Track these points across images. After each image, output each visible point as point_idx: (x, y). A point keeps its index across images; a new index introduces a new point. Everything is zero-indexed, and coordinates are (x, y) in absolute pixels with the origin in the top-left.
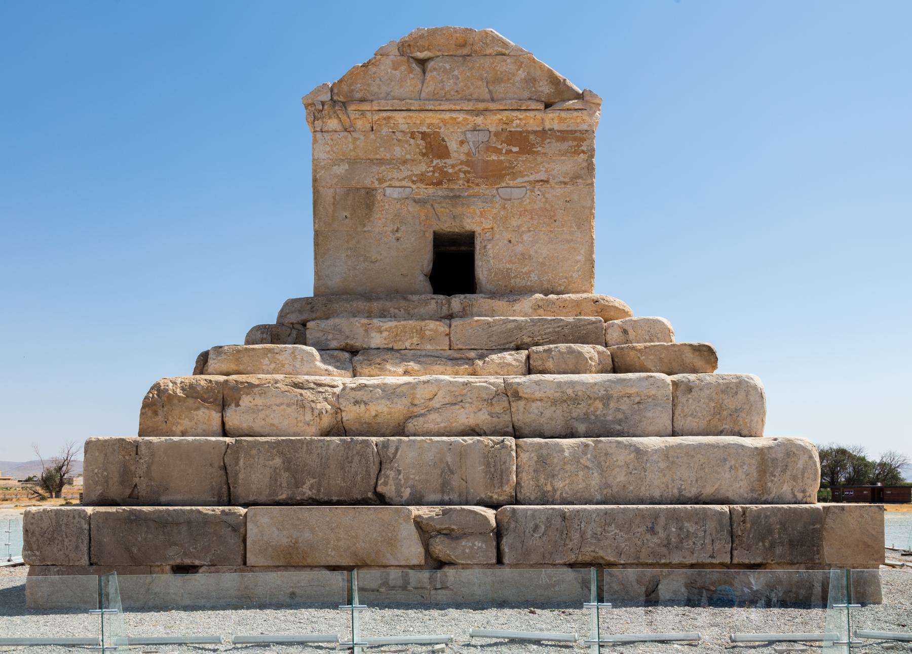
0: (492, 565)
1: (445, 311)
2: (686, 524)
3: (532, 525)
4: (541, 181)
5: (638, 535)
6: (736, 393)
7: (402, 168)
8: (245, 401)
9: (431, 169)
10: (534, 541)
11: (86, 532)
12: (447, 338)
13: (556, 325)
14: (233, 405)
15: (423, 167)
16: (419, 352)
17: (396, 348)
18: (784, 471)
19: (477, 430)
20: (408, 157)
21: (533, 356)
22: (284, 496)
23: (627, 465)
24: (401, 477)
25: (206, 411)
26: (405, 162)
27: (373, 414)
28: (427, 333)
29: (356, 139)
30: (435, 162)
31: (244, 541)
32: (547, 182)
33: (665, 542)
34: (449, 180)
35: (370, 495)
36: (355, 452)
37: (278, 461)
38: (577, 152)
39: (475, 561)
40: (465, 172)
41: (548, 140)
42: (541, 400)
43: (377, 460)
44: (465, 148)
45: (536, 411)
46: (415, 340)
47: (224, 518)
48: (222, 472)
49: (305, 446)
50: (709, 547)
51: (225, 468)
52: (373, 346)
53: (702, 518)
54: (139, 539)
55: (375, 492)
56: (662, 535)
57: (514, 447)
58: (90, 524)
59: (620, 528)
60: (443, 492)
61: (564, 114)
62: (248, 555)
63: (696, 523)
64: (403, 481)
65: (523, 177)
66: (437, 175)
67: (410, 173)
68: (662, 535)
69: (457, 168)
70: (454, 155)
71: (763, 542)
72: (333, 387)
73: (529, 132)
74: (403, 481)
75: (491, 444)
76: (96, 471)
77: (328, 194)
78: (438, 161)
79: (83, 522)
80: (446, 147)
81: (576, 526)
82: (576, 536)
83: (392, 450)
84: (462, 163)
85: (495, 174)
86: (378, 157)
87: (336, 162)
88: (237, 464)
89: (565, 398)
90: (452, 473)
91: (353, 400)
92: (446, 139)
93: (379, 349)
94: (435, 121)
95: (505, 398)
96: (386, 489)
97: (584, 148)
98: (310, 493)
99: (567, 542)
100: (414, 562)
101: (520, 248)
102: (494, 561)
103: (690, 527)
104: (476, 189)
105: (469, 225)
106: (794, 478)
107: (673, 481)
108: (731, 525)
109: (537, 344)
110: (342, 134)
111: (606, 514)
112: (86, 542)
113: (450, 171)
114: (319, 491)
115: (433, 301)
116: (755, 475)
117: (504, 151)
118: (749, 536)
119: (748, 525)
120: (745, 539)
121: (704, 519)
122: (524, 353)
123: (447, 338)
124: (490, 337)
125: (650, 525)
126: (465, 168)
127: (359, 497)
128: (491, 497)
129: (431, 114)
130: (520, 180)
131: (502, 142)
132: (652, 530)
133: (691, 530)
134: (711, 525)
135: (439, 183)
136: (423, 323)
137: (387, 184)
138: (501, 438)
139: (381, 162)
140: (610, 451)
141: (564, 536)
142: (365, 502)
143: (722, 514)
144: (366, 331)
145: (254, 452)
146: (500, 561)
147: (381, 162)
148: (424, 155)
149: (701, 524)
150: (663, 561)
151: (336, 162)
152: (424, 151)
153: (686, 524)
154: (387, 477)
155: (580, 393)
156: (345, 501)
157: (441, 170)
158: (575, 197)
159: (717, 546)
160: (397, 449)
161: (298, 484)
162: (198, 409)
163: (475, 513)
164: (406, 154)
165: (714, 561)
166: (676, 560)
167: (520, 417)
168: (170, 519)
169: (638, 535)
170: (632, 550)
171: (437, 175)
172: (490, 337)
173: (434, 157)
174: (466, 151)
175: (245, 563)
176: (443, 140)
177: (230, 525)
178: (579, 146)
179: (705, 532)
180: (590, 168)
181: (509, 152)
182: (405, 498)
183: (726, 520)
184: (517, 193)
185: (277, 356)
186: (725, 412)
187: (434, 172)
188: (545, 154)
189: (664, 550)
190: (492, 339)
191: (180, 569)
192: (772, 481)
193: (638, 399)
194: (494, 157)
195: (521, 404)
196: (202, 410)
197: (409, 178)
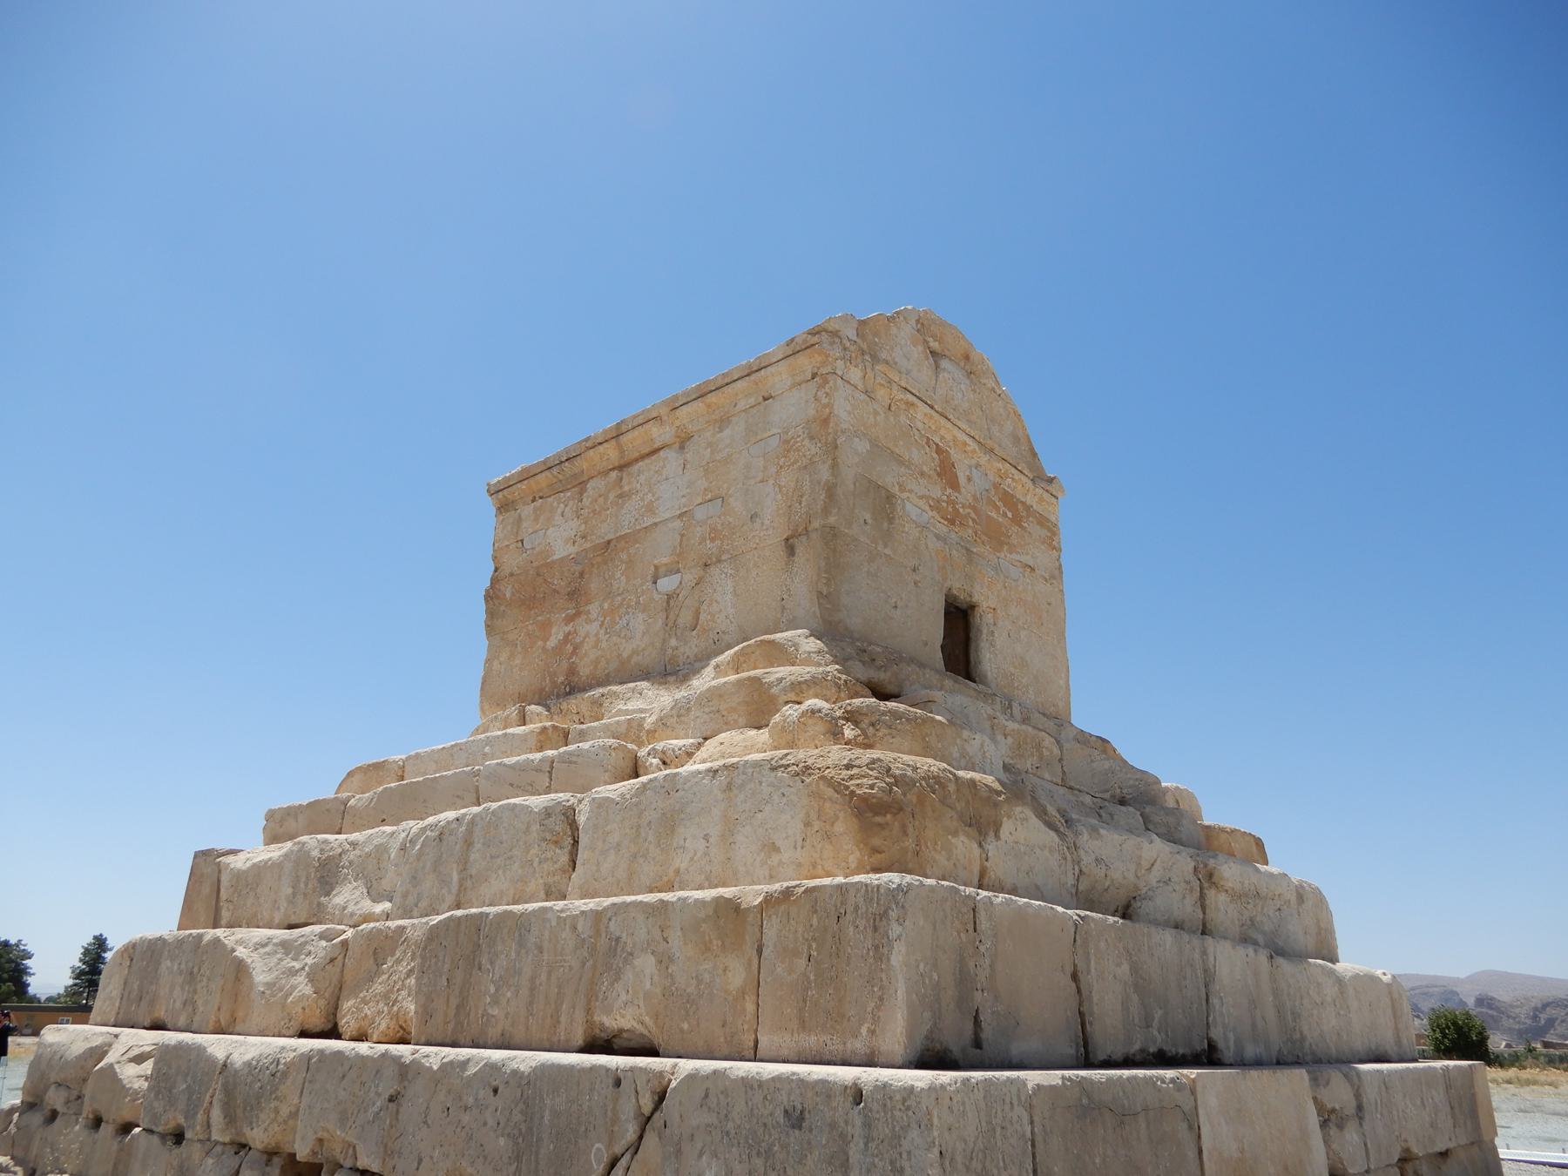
14: (992, 834)
15: (936, 492)
28: (1046, 753)
29: (876, 413)
30: (949, 491)
31: (1200, 1152)
37: (1126, 967)
51: (1075, 977)
58: (1032, 1122)
61: (1046, 495)
84: (970, 506)
85: (998, 539)
88: (1089, 972)
94: (948, 437)
129: (949, 425)
130: (1014, 556)
139: (901, 461)
148: (939, 475)
162: (955, 834)
181: (1005, 515)
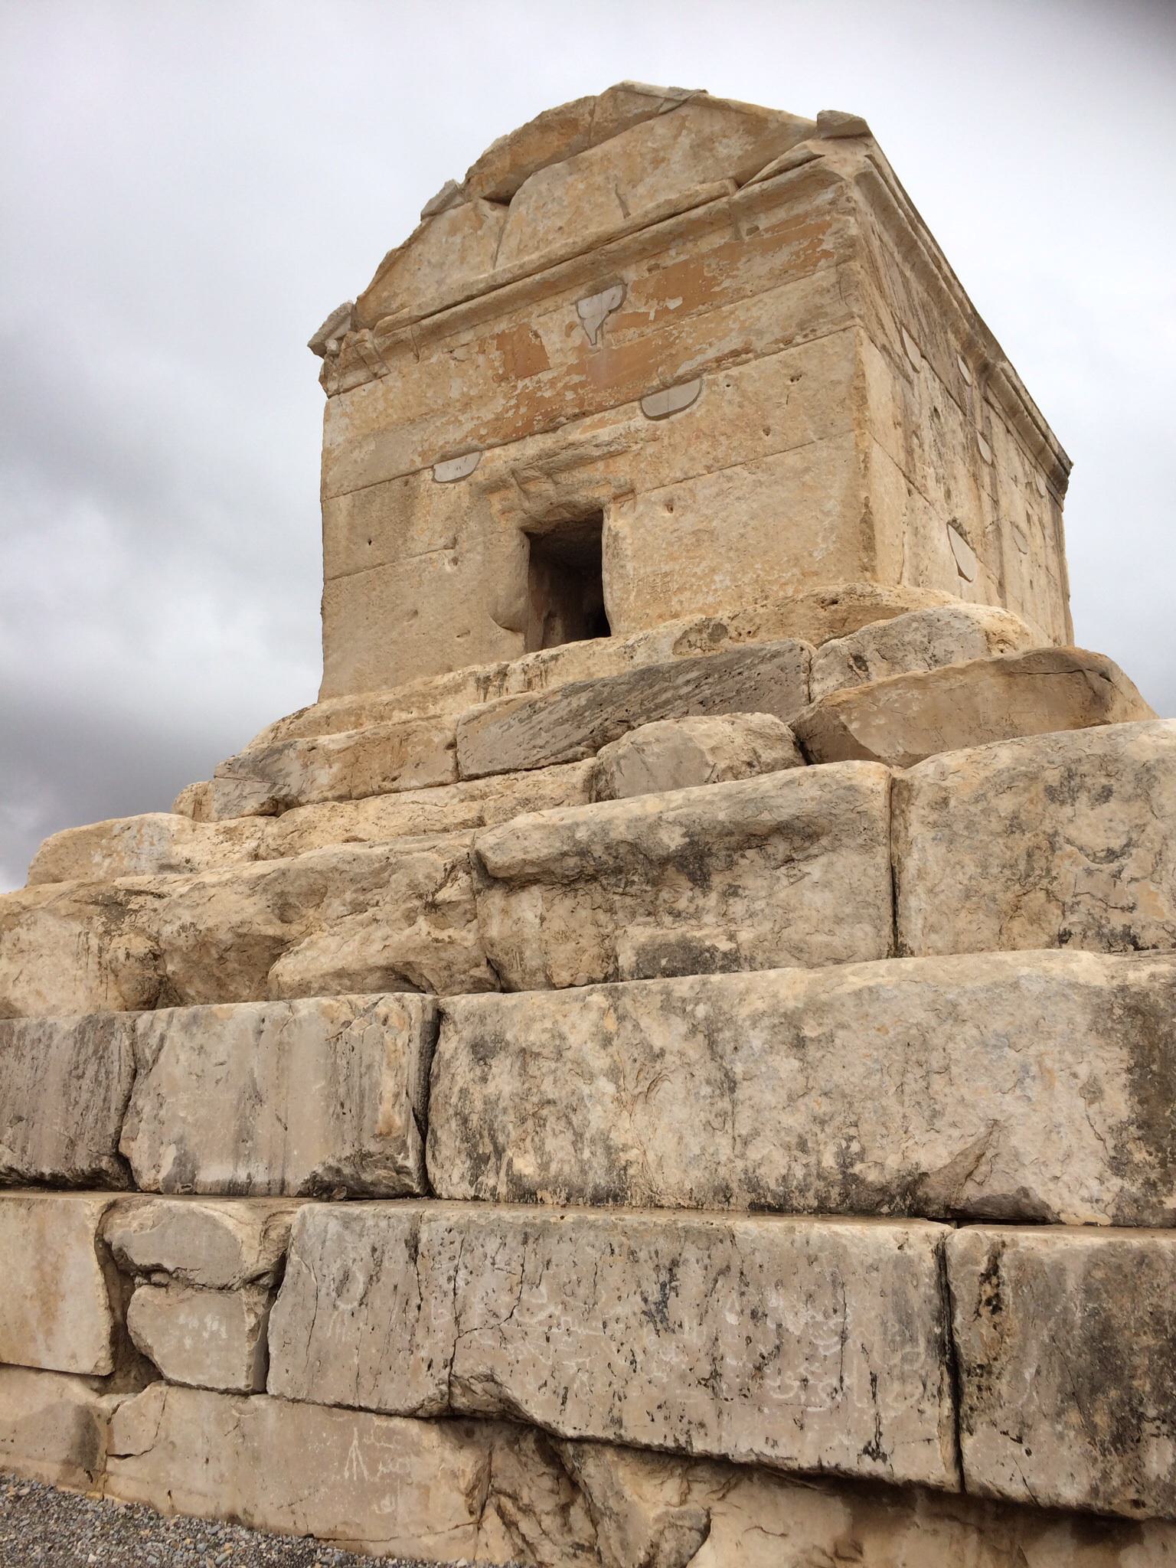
2: (775, 1300)
3: (335, 1270)
4: (735, 353)
9: (513, 402)
10: (340, 1329)
26: (466, 406)
30: (520, 384)
33: (705, 1369)
34: (545, 415)
40: (574, 388)
41: (744, 260)
44: (577, 338)
50: (861, 1403)
53: (834, 1279)
56: (693, 1335)
59: (564, 1293)
60: (237, 1156)
66: (523, 410)
68: (693, 1335)
69: (560, 385)
72: (160, 896)
73: (703, 256)
75: (345, 1014)
78: (527, 381)
80: (542, 347)
82: (441, 1314)
83: (154, 1041)
86: (424, 409)
89: (590, 870)
90: (259, 1099)
92: (540, 332)
97: (828, 245)
99: (420, 1333)
100: (86, 1366)
101: (689, 522)
105: (583, 497)
110: (370, 385)
113: (547, 394)
114: (24, 1150)
117: (652, 316)
118: (1017, 1374)
121: (837, 1283)
123: (450, 753)
124: (534, 737)
126: (576, 379)
128: (338, 1171)
131: (649, 297)
133: (794, 1326)
134: (865, 1309)
137: (438, 456)
138: (374, 997)
141: (413, 1313)
143: (904, 1265)
144: (305, 766)
148: (503, 378)
149: (828, 1302)
150: (699, 1446)
151: (354, 444)
157: (531, 399)
158: (810, 366)
159: (894, 1405)
160: (162, 1038)
163: (215, 1224)
164: (470, 387)
169: (617, 1329)
170: (600, 1387)
172: (534, 737)
173: (517, 378)
174: (578, 342)
176: (537, 335)
179: (843, 1337)
183: (922, 1294)
184: (679, 395)
189: (699, 1402)
190: (540, 742)
194: (631, 333)
195: (496, 899)
197: (473, 432)
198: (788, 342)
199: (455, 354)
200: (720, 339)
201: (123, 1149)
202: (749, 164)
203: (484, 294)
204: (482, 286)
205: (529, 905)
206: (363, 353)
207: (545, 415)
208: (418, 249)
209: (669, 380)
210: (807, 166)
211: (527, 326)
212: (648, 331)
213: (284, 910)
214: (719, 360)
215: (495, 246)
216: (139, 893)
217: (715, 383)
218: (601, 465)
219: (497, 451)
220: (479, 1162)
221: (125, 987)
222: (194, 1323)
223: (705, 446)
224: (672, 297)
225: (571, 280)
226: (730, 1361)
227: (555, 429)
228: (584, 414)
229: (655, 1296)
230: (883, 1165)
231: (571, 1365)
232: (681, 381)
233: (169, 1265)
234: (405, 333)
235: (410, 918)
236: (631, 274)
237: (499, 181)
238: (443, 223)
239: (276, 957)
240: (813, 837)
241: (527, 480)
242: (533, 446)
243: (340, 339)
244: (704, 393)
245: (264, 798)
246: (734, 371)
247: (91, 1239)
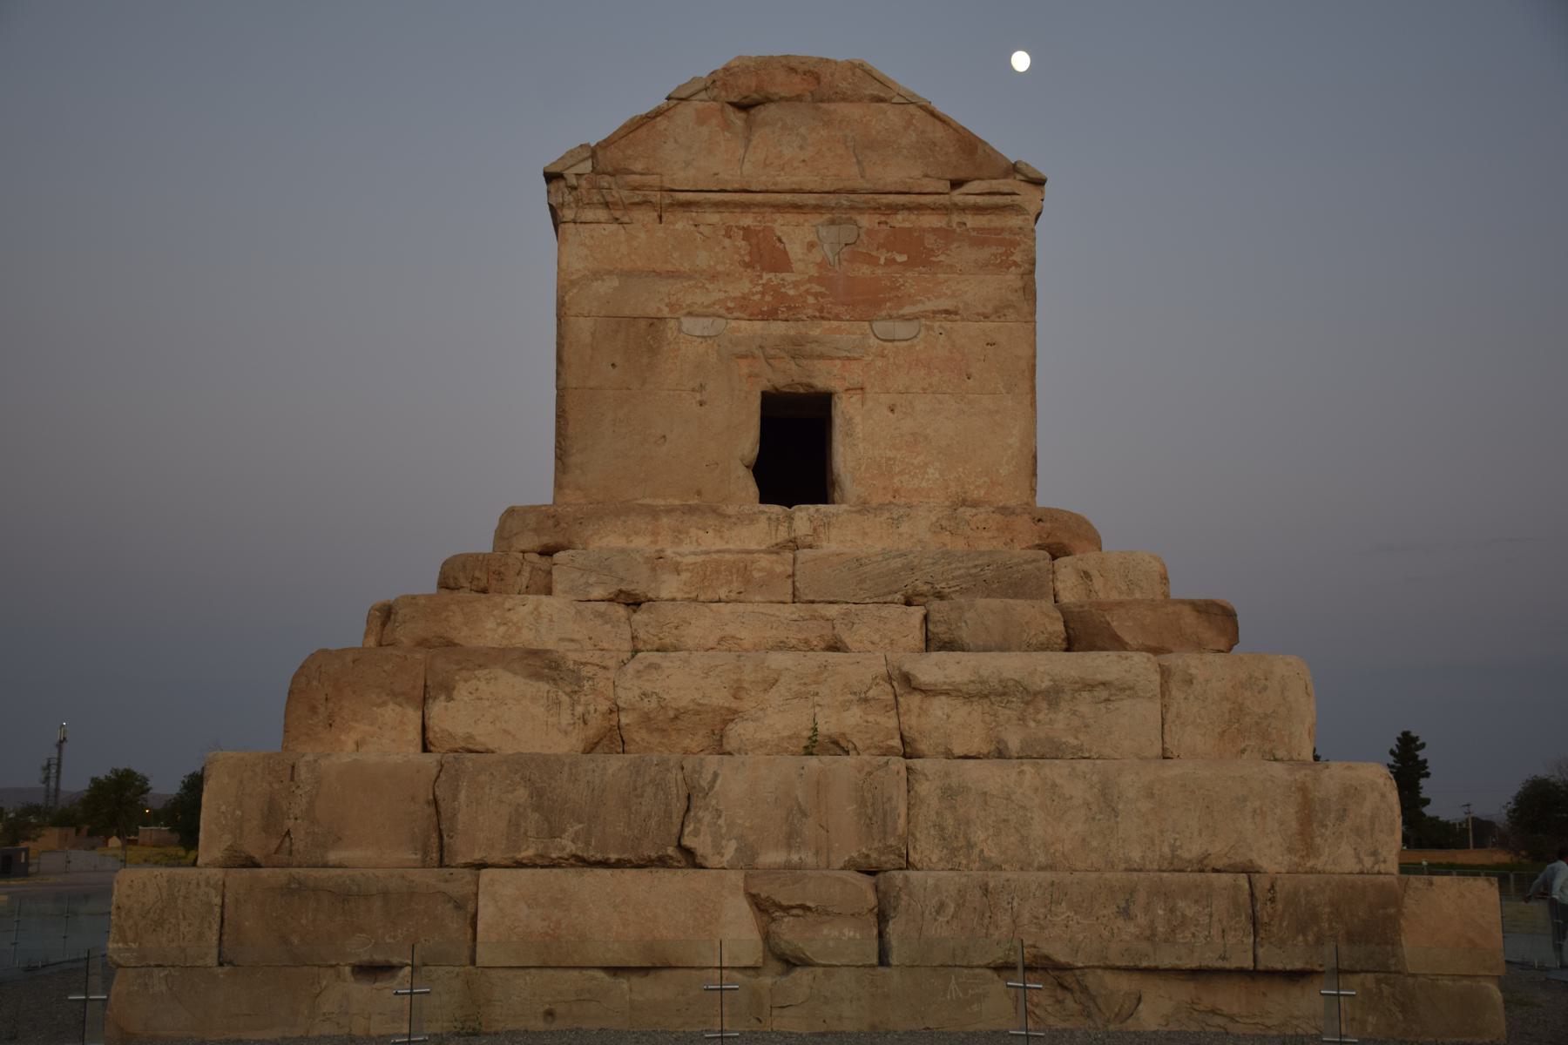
0: (872, 966)
1: (783, 535)
2: (1181, 904)
3: (935, 901)
4: (947, 312)
5: (1105, 920)
6: (1265, 688)
7: (710, 287)
8: (462, 692)
9: (759, 288)
11: (217, 910)
12: (790, 581)
13: (970, 564)
14: (443, 698)
15: (745, 286)
16: (741, 607)
17: (701, 598)
18: (1341, 818)
19: (843, 743)
20: (720, 268)
21: (935, 616)
22: (530, 852)
23: (1088, 805)
24: (721, 822)
25: (398, 709)
26: (714, 277)
27: (671, 714)
28: (756, 575)
30: (766, 276)
32: (956, 313)
33: (1148, 933)
34: (789, 308)
35: (671, 851)
36: (647, 779)
37: (522, 793)
38: (1004, 265)
39: (844, 961)
40: (816, 295)
42: (947, 693)
43: (683, 793)
44: (817, 256)
45: (939, 713)
46: (736, 586)
47: (443, 886)
48: (432, 810)
49: (566, 768)
51: (435, 801)
52: (665, 594)
54: (304, 921)
55: (680, 847)
57: (904, 773)
60: (789, 847)
62: (479, 949)
63: (1196, 902)
64: (724, 830)
65: (914, 304)
66: (768, 298)
67: (722, 295)
68: (1142, 920)
69: (802, 289)
70: (797, 266)
71: (1304, 935)
73: (924, 230)
74: (724, 830)
76: (223, 808)
77: (583, 328)
78: (772, 275)
79: (213, 893)
80: (786, 253)
81: (1005, 904)
82: (1005, 920)
83: (707, 776)
84: (810, 280)
86: (670, 267)
87: (597, 275)
88: (455, 798)
90: (805, 815)
91: (637, 692)
92: (784, 239)
93: (674, 600)
95: (888, 688)
96: (699, 843)
97: (1017, 257)
98: (573, 847)
99: (992, 930)
102: (875, 961)
103: (1186, 907)
104: (835, 324)
105: (821, 383)
106: (1358, 831)
107: (1162, 832)
108: (1253, 906)
109: (940, 596)
111: (1052, 884)
112: (216, 927)
113: (791, 292)
115: (763, 518)
116: (1294, 825)
117: (882, 261)
119: (1280, 907)
120: (1275, 930)
122: (917, 613)
123: (790, 581)
125: (1123, 905)
126: (817, 288)
127: (653, 855)
128: (868, 856)
129: (759, 197)
132: (1125, 913)
133: (1189, 913)
135: (770, 315)
136: (750, 557)
139: (674, 275)
140: (1059, 781)
142: (662, 862)
144: (653, 569)
145: (483, 778)
146: (883, 959)
147: (674, 275)
148: (747, 265)
150: (1144, 964)
152: (747, 259)
153: (1181, 904)
154: (699, 821)
155: (1011, 683)
156: (630, 861)
160: (716, 775)
161: (554, 833)
162: (385, 703)
165: (1227, 965)
166: (1167, 961)
167: (914, 721)
168: (355, 888)
169: (1105, 920)
171: (768, 298)
173: (763, 269)
174: (819, 259)
175: (473, 962)
176: (780, 240)
177: (450, 899)
178: (1008, 254)
180: (1029, 291)
181: (891, 262)
182: (727, 857)
184: (902, 329)
185: (508, 614)
186: (1247, 719)
187: (763, 294)
188: (951, 266)
191: (371, 971)
192: (1322, 836)
193: (1105, 694)
194: (865, 270)
195: (916, 699)
196: (391, 706)
198: (986, 317)
199: (701, 228)
200: (937, 298)
201: (687, 842)
202: (961, 175)
203: (735, 191)
204: (736, 186)
205: (939, 707)
206: (610, 199)
207: (789, 308)
208: (662, 123)
209: (894, 313)
210: (1008, 200)
211: (772, 230)
212: (879, 272)
213: (737, 692)
214: (935, 312)
215: (742, 151)
216: (585, 664)
217: (929, 328)
218: (838, 363)
219: (744, 324)
220: (954, 851)
221: (591, 732)
222: (836, 933)
223: (923, 372)
224: (900, 253)
225: (817, 208)
226: (1160, 929)
227: (798, 320)
228: (823, 318)
229: (1123, 905)
230: (1192, 851)
231: (1081, 937)
232: (904, 318)
233: (809, 904)
234: (656, 197)
235: (845, 706)
236: (865, 221)
237: (745, 97)
238: (687, 112)
239: (726, 722)
240: (1124, 690)
241: (774, 357)
242: (778, 328)
243: (578, 175)
244: (921, 335)
245: (614, 589)
246: (948, 325)
247: (742, 892)
